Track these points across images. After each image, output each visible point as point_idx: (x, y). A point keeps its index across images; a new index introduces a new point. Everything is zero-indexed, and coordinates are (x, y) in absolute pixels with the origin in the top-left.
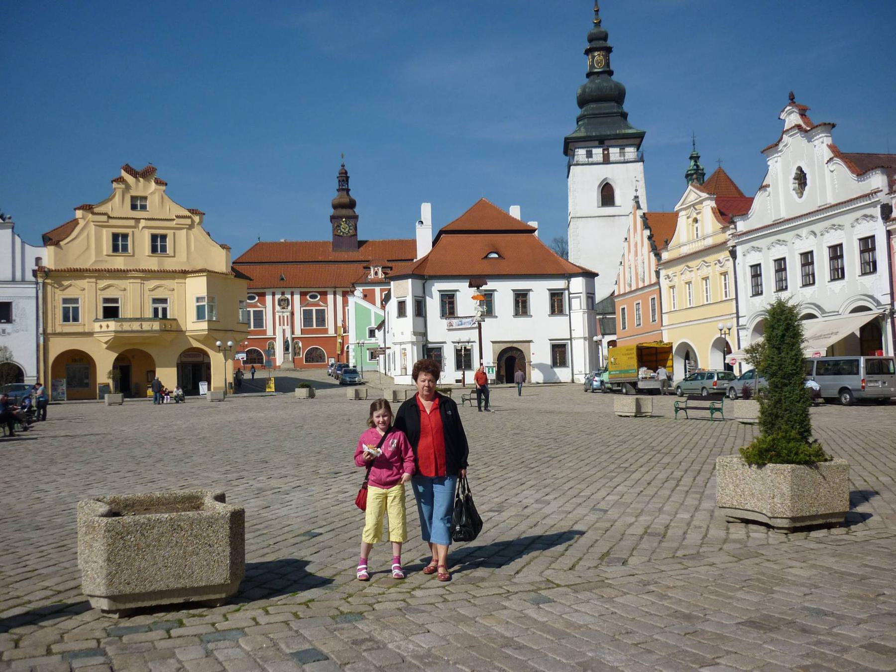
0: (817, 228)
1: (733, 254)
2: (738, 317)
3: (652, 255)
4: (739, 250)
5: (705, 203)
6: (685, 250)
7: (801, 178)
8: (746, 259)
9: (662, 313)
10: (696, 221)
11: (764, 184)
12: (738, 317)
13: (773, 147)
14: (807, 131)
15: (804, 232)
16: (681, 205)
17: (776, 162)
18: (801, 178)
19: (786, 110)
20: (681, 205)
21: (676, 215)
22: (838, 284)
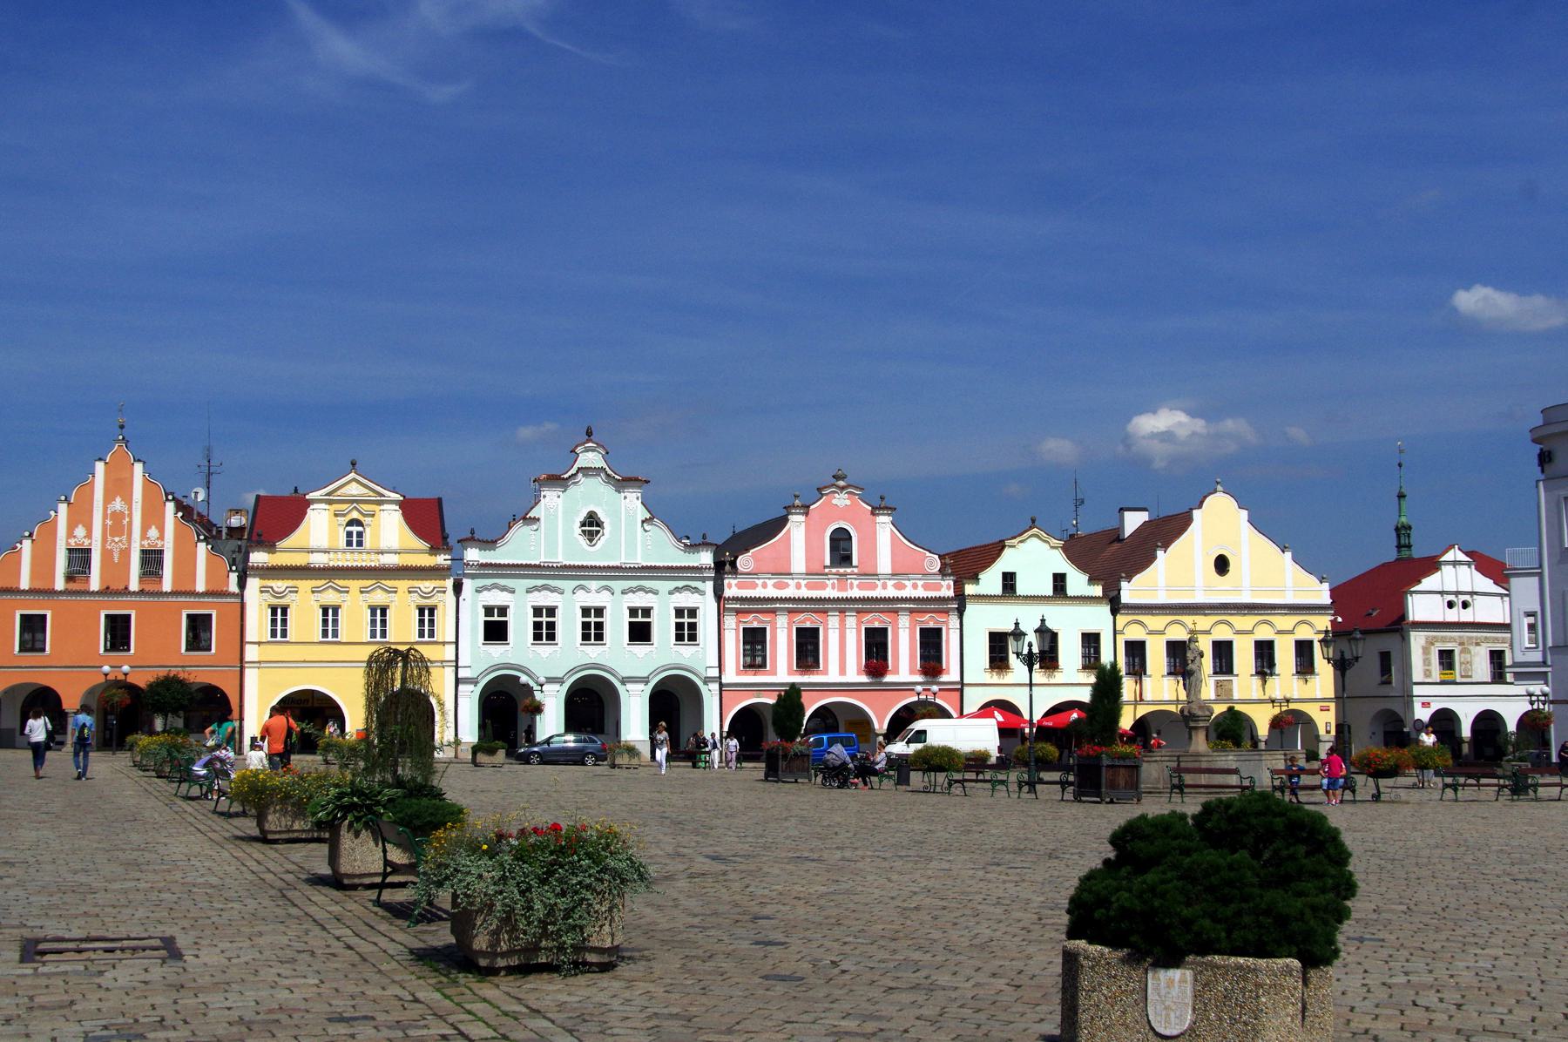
0: (618, 585)
1: (458, 588)
2: (457, 667)
3: (202, 548)
4: (468, 585)
5: (386, 507)
6: (319, 560)
7: (592, 525)
8: (476, 601)
9: (242, 643)
10: (358, 523)
11: (531, 514)
12: (457, 667)
13: (558, 480)
14: (623, 483)
15: (594, 585)
16: (326, 495)
17: (559, 497)
18: (592, 525)
19: (586, 445)
20: (326, 495)
21: (308, 503)
22: (640, 649)
